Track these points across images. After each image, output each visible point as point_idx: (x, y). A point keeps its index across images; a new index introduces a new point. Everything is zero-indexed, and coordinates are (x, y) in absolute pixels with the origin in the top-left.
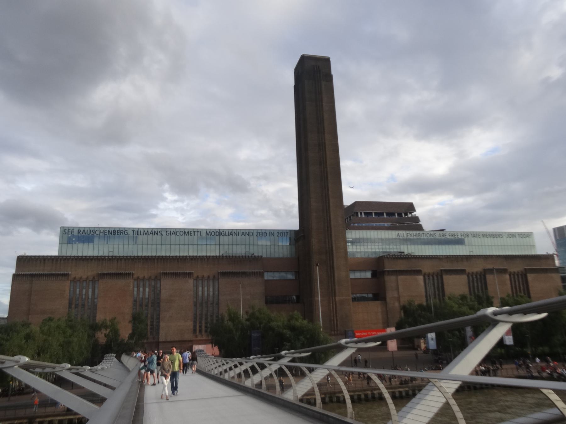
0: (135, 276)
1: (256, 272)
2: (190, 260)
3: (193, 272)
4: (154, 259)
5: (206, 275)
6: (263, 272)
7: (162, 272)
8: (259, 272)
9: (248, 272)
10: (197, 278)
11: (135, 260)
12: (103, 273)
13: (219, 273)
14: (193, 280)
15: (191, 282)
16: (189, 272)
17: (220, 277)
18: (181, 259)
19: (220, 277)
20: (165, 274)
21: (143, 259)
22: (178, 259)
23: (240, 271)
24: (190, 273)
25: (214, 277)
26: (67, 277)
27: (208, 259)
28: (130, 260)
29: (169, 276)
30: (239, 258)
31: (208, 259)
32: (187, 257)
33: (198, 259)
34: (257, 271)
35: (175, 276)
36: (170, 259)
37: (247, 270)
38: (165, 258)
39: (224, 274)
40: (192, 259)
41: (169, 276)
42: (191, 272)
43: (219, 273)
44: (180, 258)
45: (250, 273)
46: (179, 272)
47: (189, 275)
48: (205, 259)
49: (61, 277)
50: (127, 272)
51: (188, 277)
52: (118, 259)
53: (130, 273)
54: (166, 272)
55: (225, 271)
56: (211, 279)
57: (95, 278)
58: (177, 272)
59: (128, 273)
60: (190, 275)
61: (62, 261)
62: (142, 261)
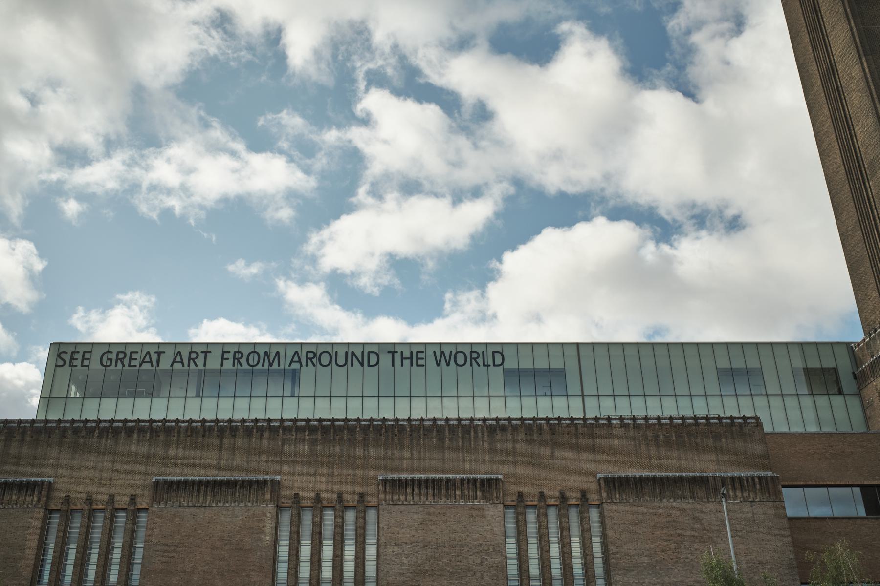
0: (286, 494)
1: (747, 478)
2: (486, 433)
3: (500, 476)
4: (351, 430)
5: (552, 489)
6: (772, 478)
7: (380, 477)
8: (760, 478)
9: (714, 478)
10: (519, 504)
11: (284, 433)
12: (165, 482)
14: (501, 507)
16: (485, 476)
17: (604, 495)
18: (452, 429)
21: (313, 430)
22: (440, 430)
24: (489, 480)
25: (584, 495)
26: (36, 495)
27: (552, 429)
28: (266, 434)
29: (409, 491)
30: (671, 425)
31: (552, 429)
32: (476, 423)
33: (515, 428)
36: (413, 429)
40: (492, 430)
41: (409, 491)
42: (493, 476)
43: (602, 482)
44: (449, 426)
46: (448, 480)
47: (488, 487)
48: (540, 428)
49: (15, 494)
50: (254, 478)
51: (484, 495)
52: (222, 430)
53: (265, 482)
54: (395, 476)
55: (623, 475)
57: (139, 499)
58: (441, 480)
59: (257, 482)
60: (490, 487)
61: (28, 439)
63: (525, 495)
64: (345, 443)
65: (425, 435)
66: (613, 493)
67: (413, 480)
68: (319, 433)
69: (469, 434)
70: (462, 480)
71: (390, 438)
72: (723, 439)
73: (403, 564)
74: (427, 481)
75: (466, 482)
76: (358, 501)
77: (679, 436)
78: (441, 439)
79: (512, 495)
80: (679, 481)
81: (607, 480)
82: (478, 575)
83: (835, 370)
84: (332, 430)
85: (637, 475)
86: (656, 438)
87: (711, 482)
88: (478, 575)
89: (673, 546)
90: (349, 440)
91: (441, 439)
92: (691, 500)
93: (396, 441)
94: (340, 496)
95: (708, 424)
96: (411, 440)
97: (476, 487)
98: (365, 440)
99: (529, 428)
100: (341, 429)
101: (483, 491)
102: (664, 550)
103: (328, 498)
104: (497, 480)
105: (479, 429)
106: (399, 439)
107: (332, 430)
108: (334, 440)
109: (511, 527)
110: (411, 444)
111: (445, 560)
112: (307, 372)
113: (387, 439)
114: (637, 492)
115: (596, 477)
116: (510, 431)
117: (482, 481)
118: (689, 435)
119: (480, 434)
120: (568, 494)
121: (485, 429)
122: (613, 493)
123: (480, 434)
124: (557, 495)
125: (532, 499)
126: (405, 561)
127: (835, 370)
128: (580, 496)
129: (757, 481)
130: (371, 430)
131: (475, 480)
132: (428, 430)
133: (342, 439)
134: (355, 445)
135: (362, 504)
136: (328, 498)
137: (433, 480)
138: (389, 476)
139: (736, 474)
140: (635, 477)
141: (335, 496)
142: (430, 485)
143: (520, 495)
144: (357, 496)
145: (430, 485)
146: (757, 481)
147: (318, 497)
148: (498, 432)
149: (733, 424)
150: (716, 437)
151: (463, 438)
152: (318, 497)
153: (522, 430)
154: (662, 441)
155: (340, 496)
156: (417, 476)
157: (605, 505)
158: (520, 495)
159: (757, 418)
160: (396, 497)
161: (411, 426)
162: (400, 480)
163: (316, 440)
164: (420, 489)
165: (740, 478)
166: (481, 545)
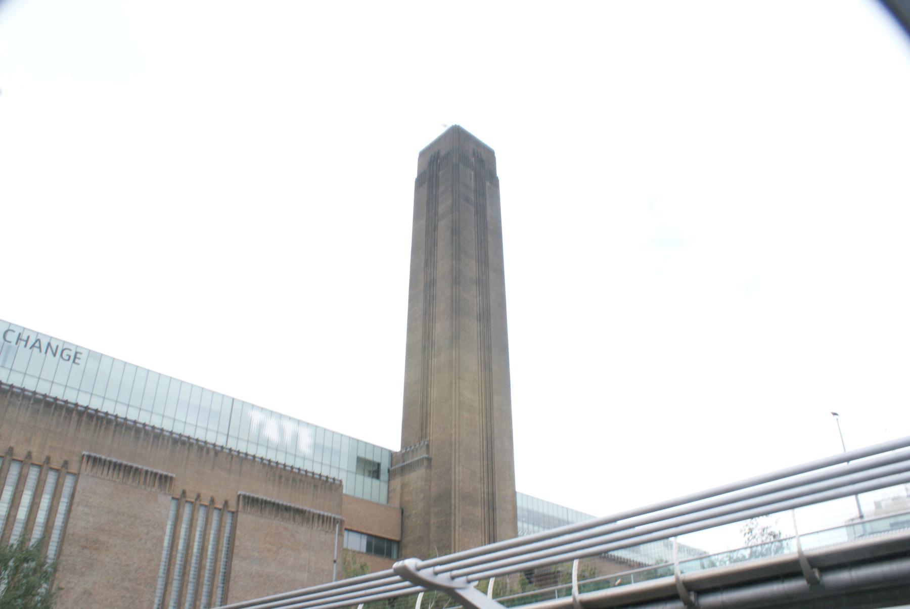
2: (170, 443)
3: (174, 476)
7: (86, 453)
9: (309, 512)
10: (180, 500)
13: (241, 497)
14: (170, 498)
15: (165, 506)
17: (241, 506)
18: (147, 433)
19: (241, 506)
20: (96, 461)
23: (293, 505)
24: (166, 477)
25: (226, 503)
27: (217, 453)
30: (292, 471)
32: (165, 433)
33: (191, 445)
34: (329, 514)
35: (121, 475)
36: (118, 424)
37: (306, 508)
38: (102, 418)
39: (252, 502)
40: (175, 441)
43: (241, 497)
45: (314, 514)
46: (137, 469)
47: (164, 480)
48: (208, 450)
54: (98, 456)
55: (256, 496)
56: (216, 508)
58: (131, 467)
60: (166, 481)
62: (31, 405)
63: (188, 493)
64: (62, 418)
65: (126, 430)
66: (246, 506)
67: (110, 462)
68: (42, 405)
69: (158, 439)
70: (147, 472)
71: (99, 425)
72: (319, 489)
73: (89, 522)
74: (121, 465)
75: (149, 473)
76: (63, 466)
77: (294, 480)
78: (137, 437)
79: (178, 493)
80: (288, 509)
81: (244, 497)
82: (143, 541)
83: (379, 465)
84: (54, 406)
85: (265, 498)
86: (281, 477)
87: (307, 513)
88: (143, 541)
89: (275, 549)
90: (65, 418)
91: (137, 437)
92: (293, 523)
93: (103, 427)
94: (48, 459)
95: (313, 477)
96: (115, 431)
97: (155, 479)
98: (79, 422)
99: (201, 448)
100: (61, 407)
101: (160, 483)
102: (269, 550)
103: (37, 458)
104: (171, 478)
105: (166, 438)
106: (106, 428)
107: (54, 406)
108: (53, 414)
109: (172, 513)
110: (114, 435)
111: (122, 525)
112: (24, 352)
113: (96, 425)
114: (261, 509)
115: (237, 492)
116: (188, 445)
117: (161, 476)
118: (300, 481)
119: (166, 442)
120: (216, 500)
121: (170, 441)
122: (246, 506)
123: (166, 442)
124: (209, 499)
125: (191, 497)
126: (91, 519)
127: (379, 465)
128: (223, 503)
129: (332, 520)
130: (85, 415)
131: (156, 474)
132: (129, 428)
133: (60, 415)
134: (70, 422)
135: (63, 470)
136: (37, 458)
137: (126, 466)
138: (93, 454)
139: (322, 513)
140: (262, 500)
141: (44, 458)
142: (122, 469)
143: (184, 493)
144: (62, 462)
145: (122, 469)
146: (332, 520)
147: (29, 455)
148: (179, 444)
149: (327, 481)
150: (316, 486)
151: (153, 441)
152: (29, 455)
153: (196, 447)
154: (283, 480)
155: (48, 459)
156: (114, 460)
157: (239, 513)
158: (184, 493)
159: (341, 481)
160: (95, 470)
161: (117, 422)
162: (100, 459)
163: (38, 410)
164: (114, 469)
165: (323, 516)
166: (150, 521)
